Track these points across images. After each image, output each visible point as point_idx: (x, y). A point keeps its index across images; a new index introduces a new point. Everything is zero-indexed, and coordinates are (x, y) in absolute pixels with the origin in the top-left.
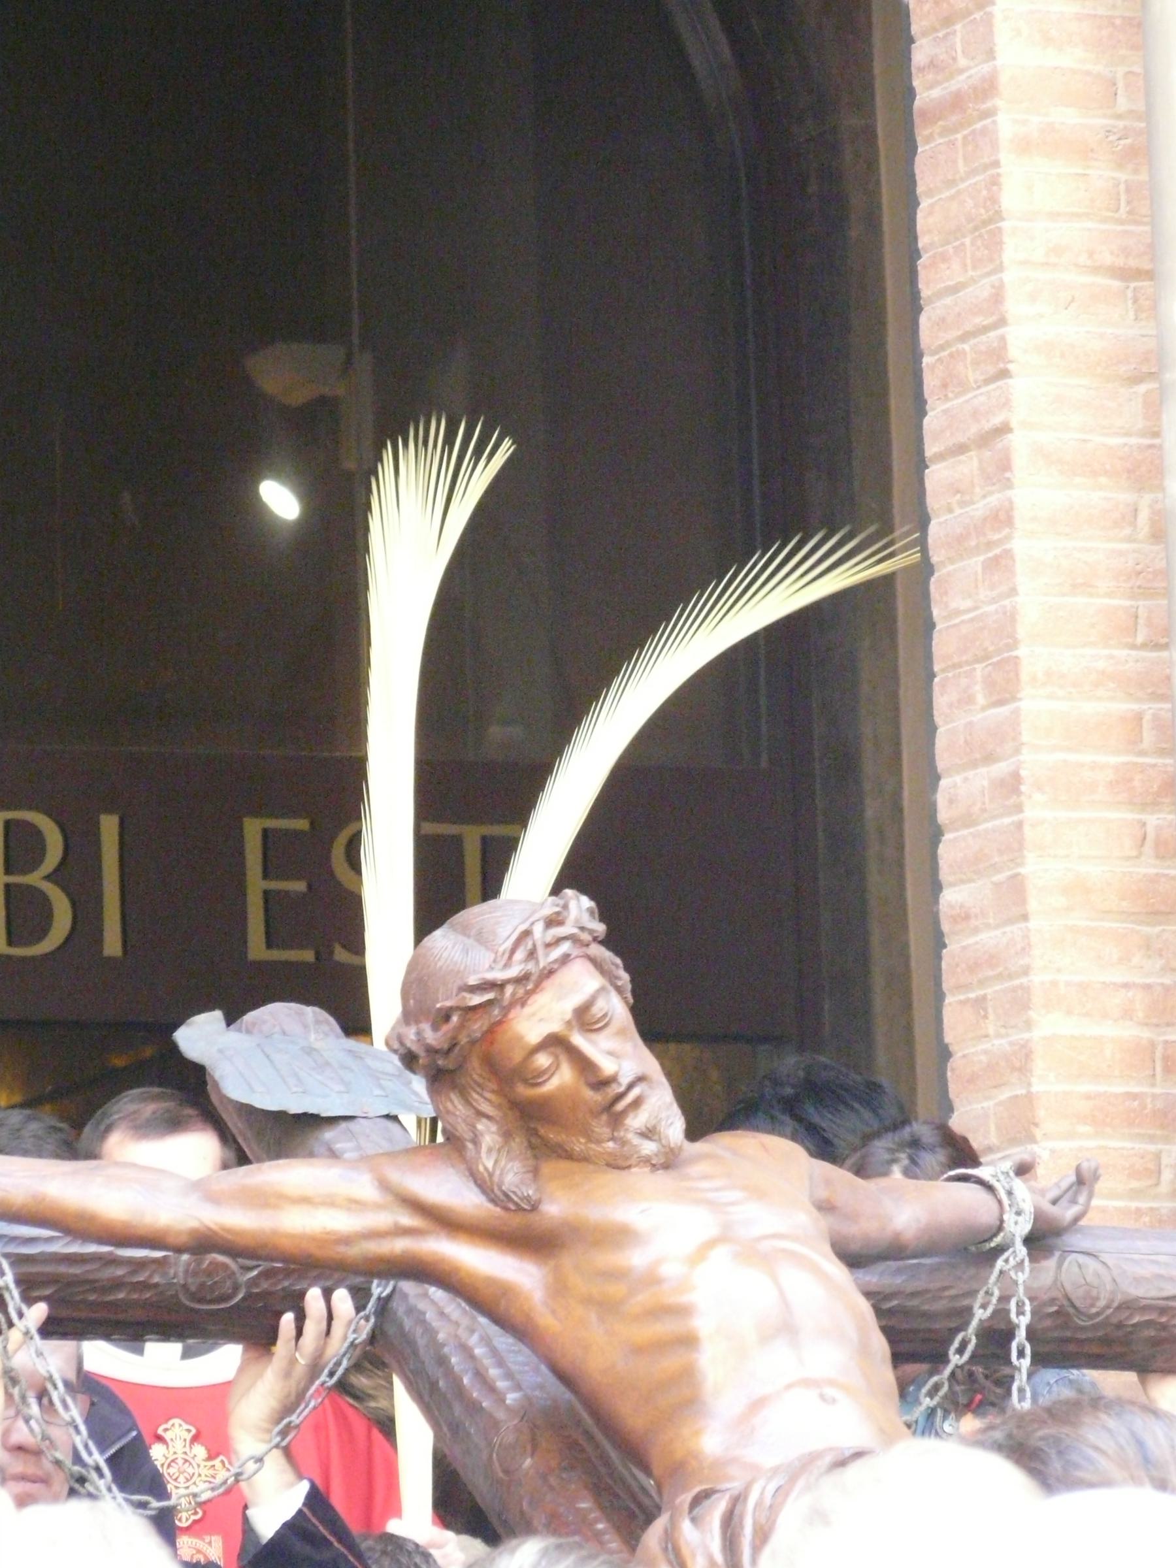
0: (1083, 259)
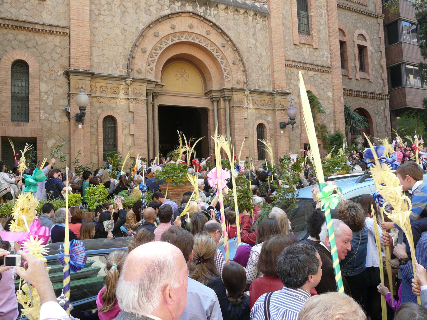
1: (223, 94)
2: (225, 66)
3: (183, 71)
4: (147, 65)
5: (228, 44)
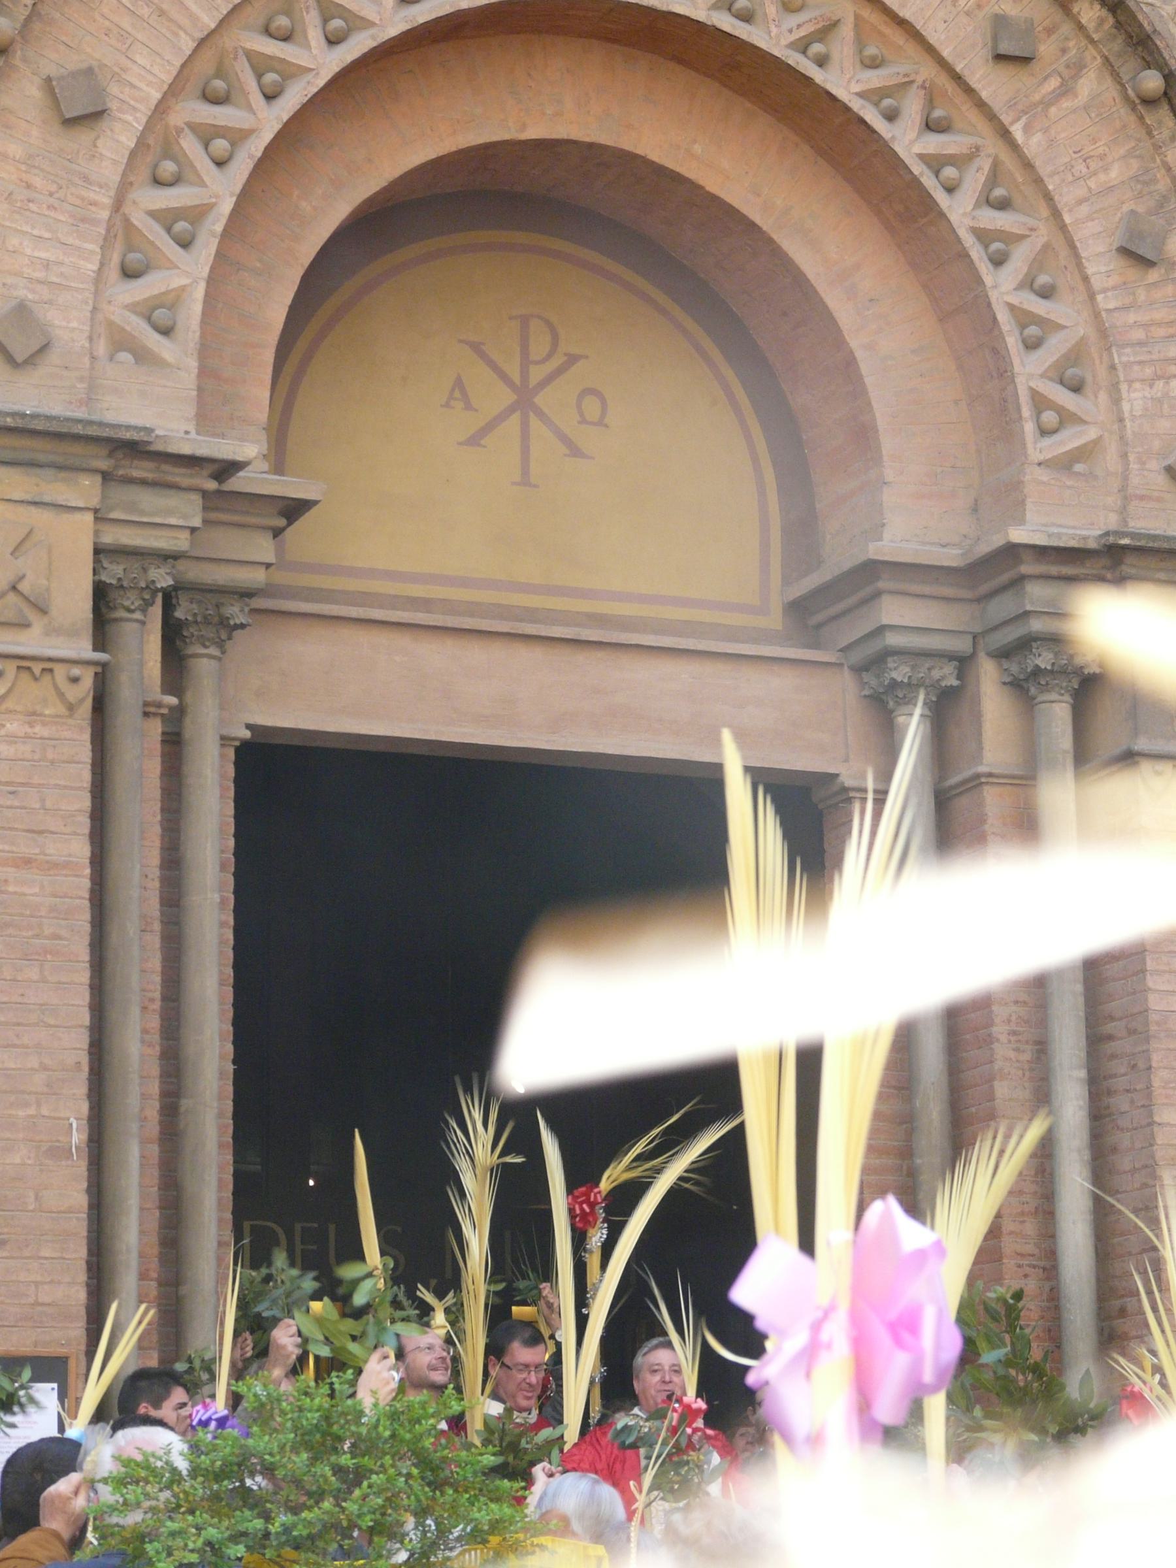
1: (1002, 607)
2: (1028, 283)
3: (539, 345)
4: (113, 273)
5: (1066, 28)
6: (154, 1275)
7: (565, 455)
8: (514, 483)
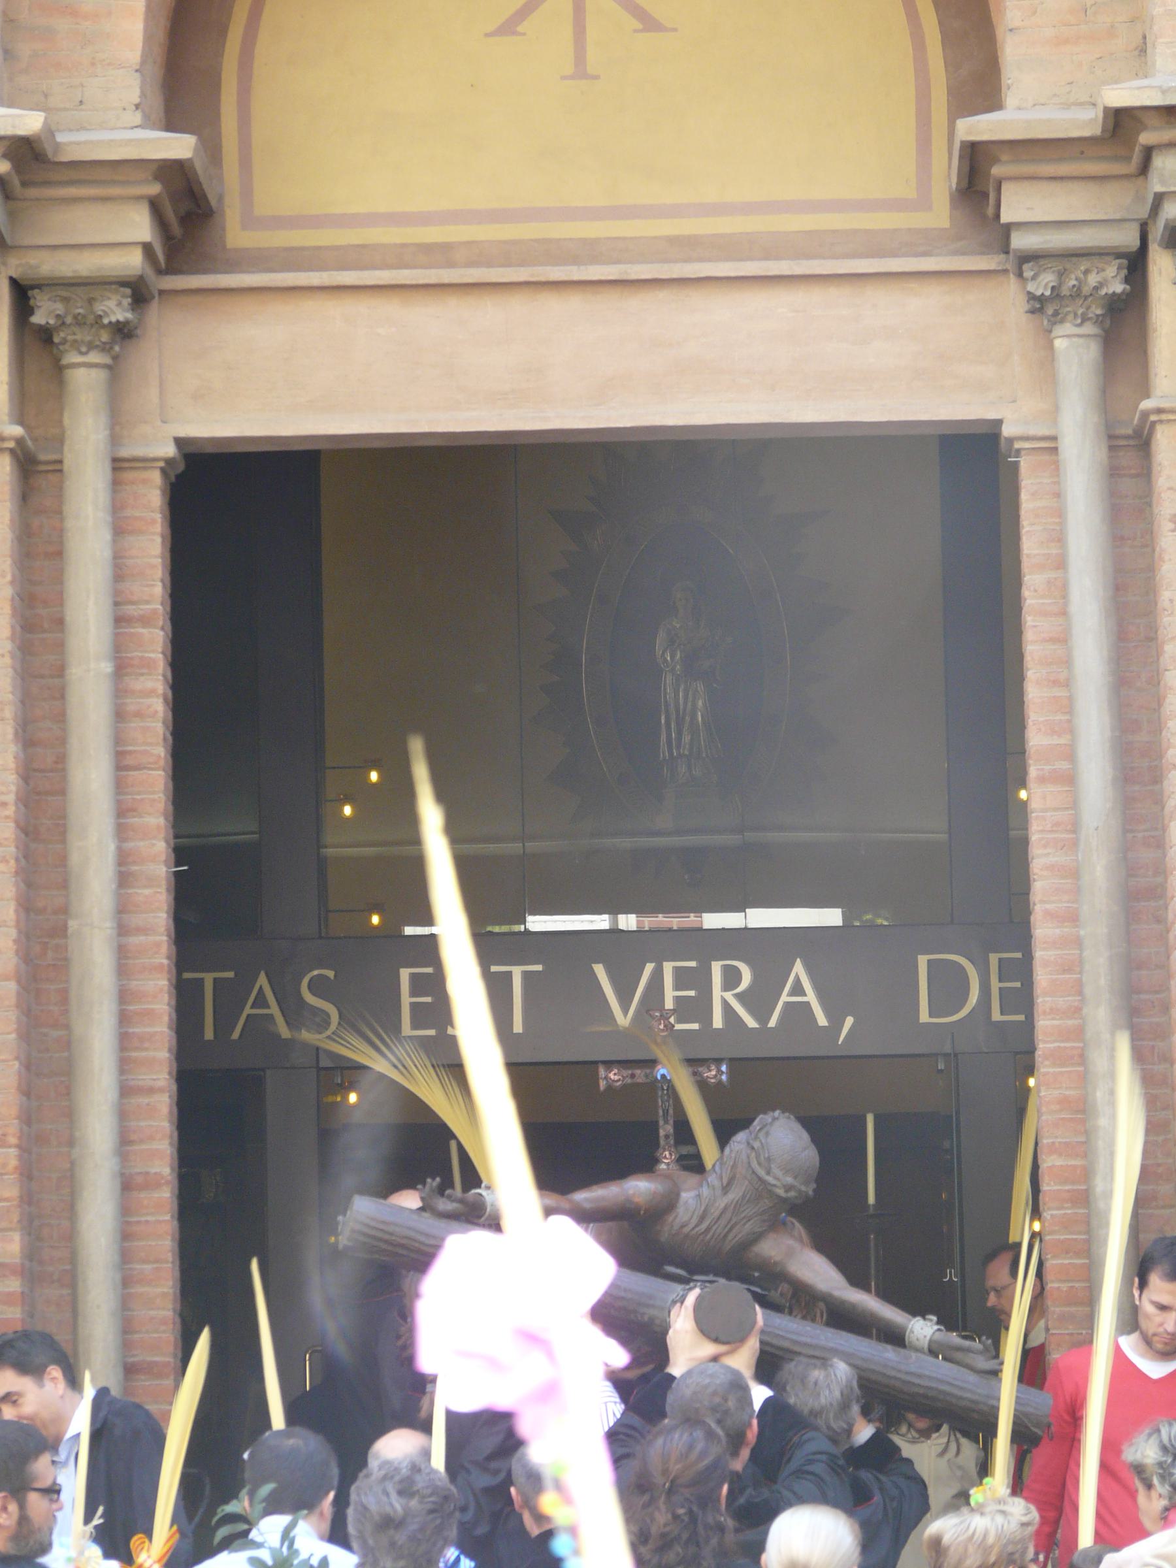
0: (1069, 827)
6: (13, 1140)
7: (636, 31)
8: (564, 78)
